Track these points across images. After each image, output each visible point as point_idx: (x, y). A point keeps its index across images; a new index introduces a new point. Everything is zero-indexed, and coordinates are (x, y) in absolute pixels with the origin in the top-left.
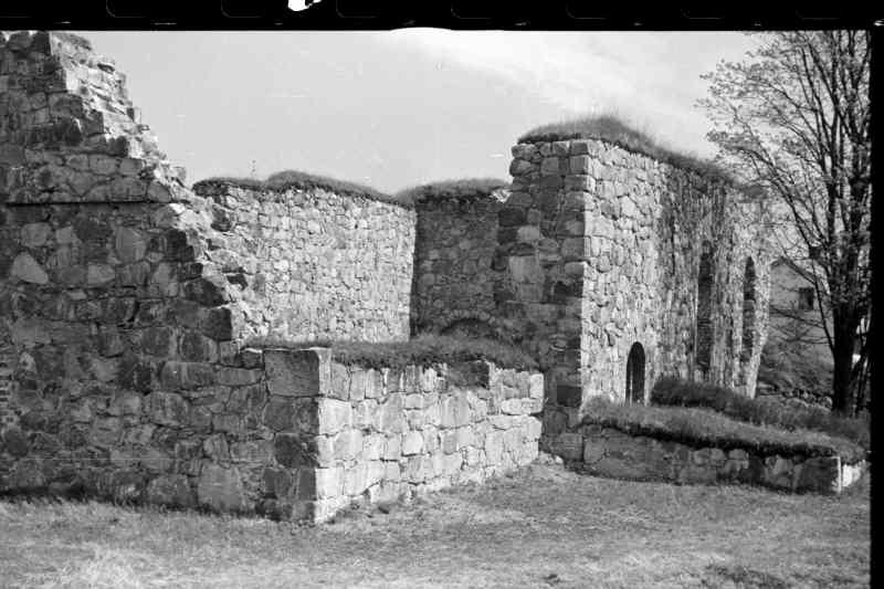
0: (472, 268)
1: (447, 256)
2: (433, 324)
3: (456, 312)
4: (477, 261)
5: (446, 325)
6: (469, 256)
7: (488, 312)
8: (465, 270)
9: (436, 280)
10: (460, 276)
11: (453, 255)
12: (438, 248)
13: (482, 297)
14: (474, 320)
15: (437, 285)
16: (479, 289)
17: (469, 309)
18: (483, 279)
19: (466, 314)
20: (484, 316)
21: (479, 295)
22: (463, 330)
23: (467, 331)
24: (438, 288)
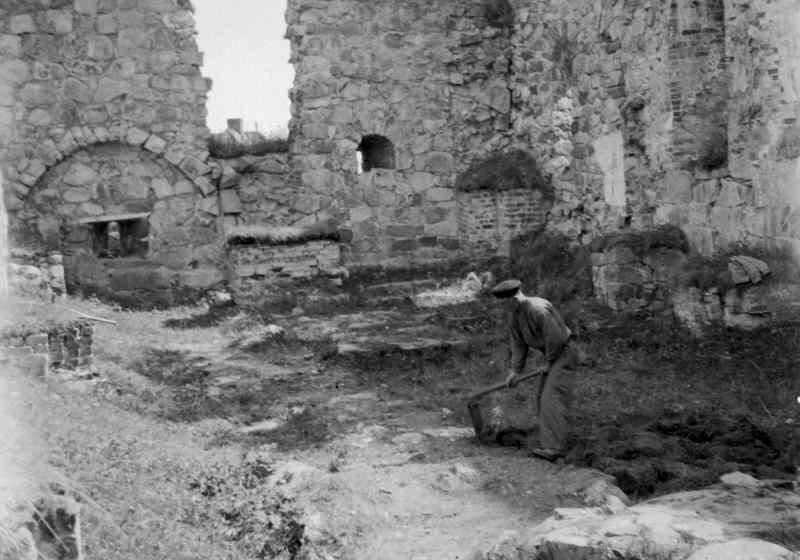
0: (106, 51)
1: (51, 24)
2: (30, 156)
3: (78, 133)
4: (113, 35)
5: (60, 156)
6: (95, 28)
7: (144, 127)
8: (91, 53)
9: (31, 72)
10: (83, 63)
11: (62, 22)
12: (29, 11)
13: (129, 102)
14: (114, 145)
15: (34, 81)
16: (123, 87)
17: (107, 122)
18: (129, 68)
19: (101, 134)
20: (136, 137)
21: (123, 97)
22: (89, 165)
23: (95, 166)
24: (37, 87)
